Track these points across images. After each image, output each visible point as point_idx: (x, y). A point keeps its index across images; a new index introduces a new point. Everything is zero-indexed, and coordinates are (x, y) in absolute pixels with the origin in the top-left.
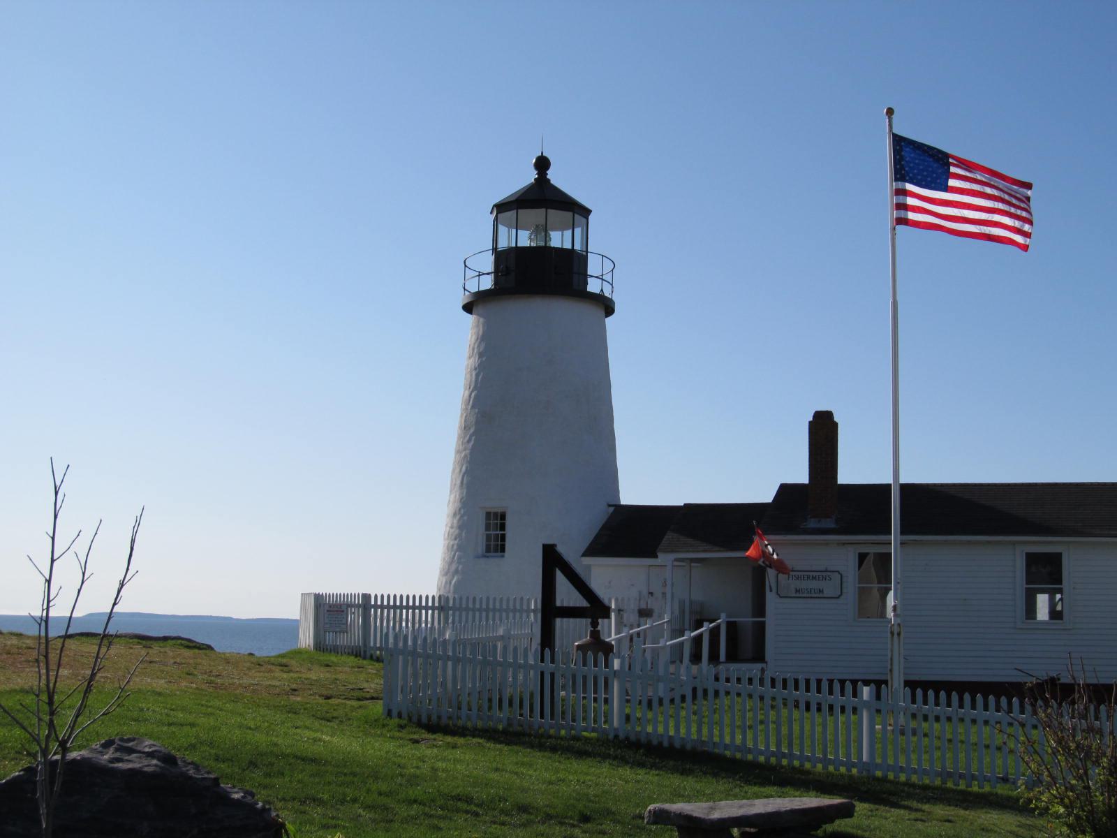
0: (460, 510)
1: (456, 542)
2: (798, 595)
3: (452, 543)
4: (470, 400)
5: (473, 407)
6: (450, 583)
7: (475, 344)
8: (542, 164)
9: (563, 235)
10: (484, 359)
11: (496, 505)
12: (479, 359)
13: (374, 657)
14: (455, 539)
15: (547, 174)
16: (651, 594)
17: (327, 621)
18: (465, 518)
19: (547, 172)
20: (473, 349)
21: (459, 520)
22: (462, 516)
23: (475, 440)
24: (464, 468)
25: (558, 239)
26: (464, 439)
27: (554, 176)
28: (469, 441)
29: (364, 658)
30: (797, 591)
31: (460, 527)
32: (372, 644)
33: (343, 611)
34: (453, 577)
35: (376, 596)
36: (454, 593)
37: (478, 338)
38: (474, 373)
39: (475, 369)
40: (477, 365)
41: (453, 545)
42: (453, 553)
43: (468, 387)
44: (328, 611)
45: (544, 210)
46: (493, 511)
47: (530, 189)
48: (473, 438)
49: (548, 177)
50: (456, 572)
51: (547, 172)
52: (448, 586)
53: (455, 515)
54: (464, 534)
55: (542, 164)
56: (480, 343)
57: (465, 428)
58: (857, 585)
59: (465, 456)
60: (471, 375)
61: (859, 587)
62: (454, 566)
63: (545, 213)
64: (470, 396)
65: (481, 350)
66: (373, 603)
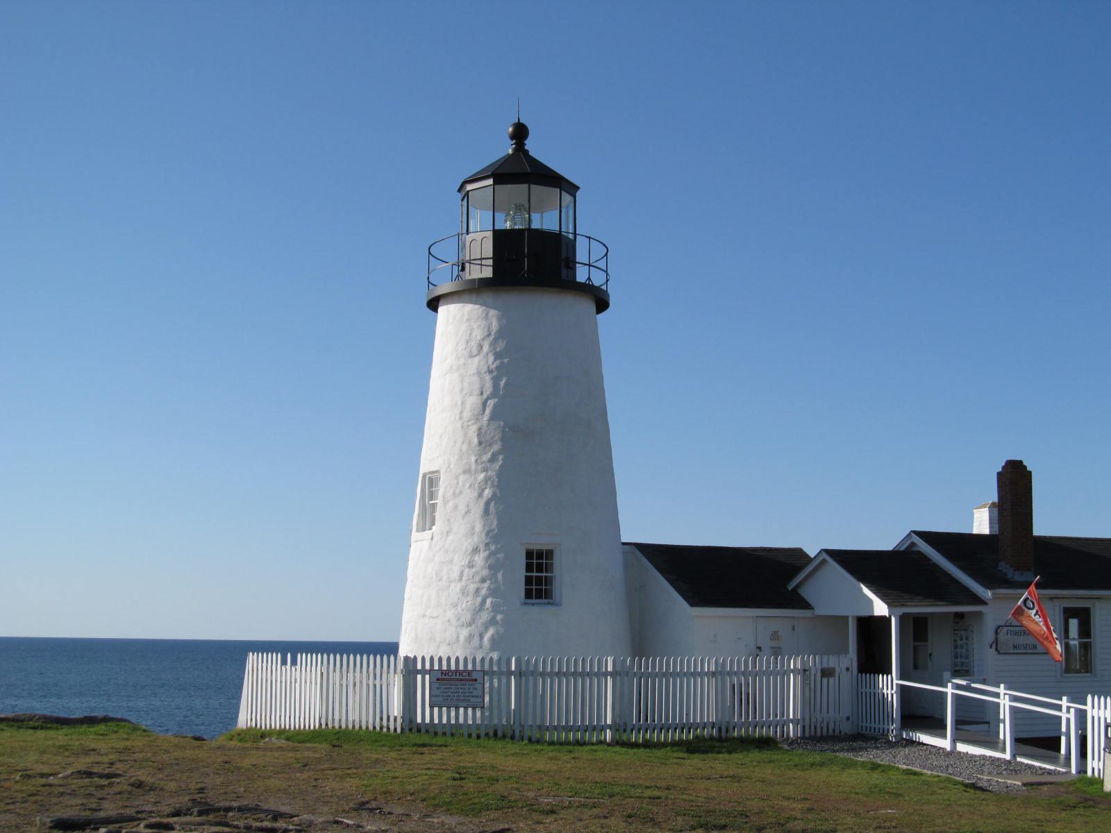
0: (487, 545)
1: (486, 585)
2: (1015, 651)
3: (473, 587)
4: (484, 410)
5: (493, 417)
6: (481, 636)
7: (483, 340)
8: (520, 133)
9: (542, 217)
10: (506, 360)
11: (540, 542)
12: (495, 360)
13: (534, 739)
14: (483, 581)
15: (525, 145)
16: (759, 648)
17: (437, 692)
18: (501, 556)
19: (525, 142)
20: (481, 347)
21: (487, 559)
22: (492, 554)
23: (503, 460)
24: (487, 493)
25: (546, 221)
26: (480, 455)
27: (531, 145)
28: (493, 459)
29: (570, 745)
30: (1015, 647)
31: (493, 568)
32: (419, 720)
33: (476, 680)
34: (487, 629)
35: (423, 659)
36: (493, 649)
37: (489, 335)
38: (488, 378)
39: (490, 372)
40: (493, 367)
41: (477, 590)
42: (479, 599)
43: (477, 392)
44: (438, 679)
45: (526, 186)
46: (535, 548)
47: (508, 159)
48: (501, 457)
49: (526, 147)
50: (492, 622)
51: (525, 142)
52: (477, 638)
53: (476, 550)
54: (500, 575)
55: (520, 133)
56: (495, 340)
57: (480, 443)
58: (1091, 640)
59: (486, 480)
60: (482, 379)
61: (1090, 638)
62: (485, 616)
63: (527, 189)
64: (484, 404)
65: (498, 349)
66: (419, 667)
